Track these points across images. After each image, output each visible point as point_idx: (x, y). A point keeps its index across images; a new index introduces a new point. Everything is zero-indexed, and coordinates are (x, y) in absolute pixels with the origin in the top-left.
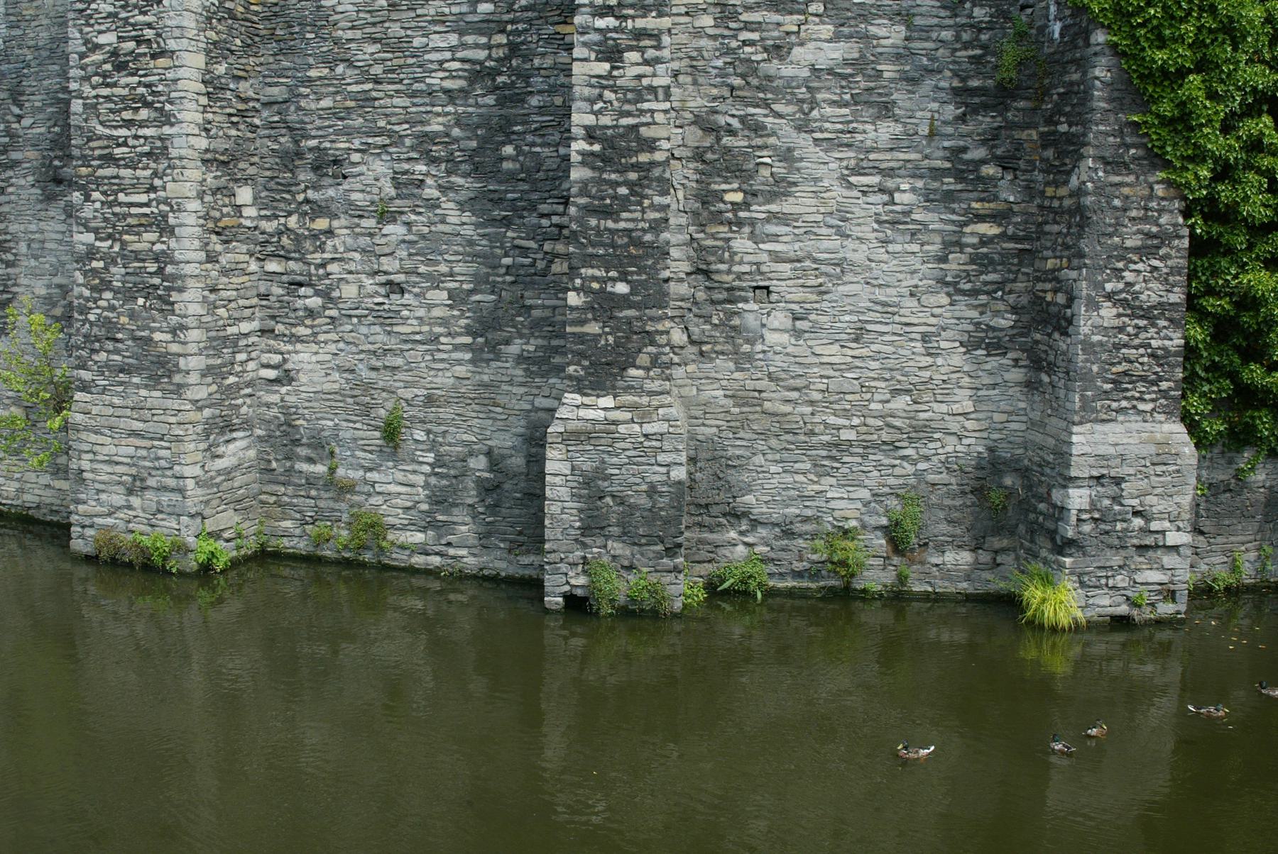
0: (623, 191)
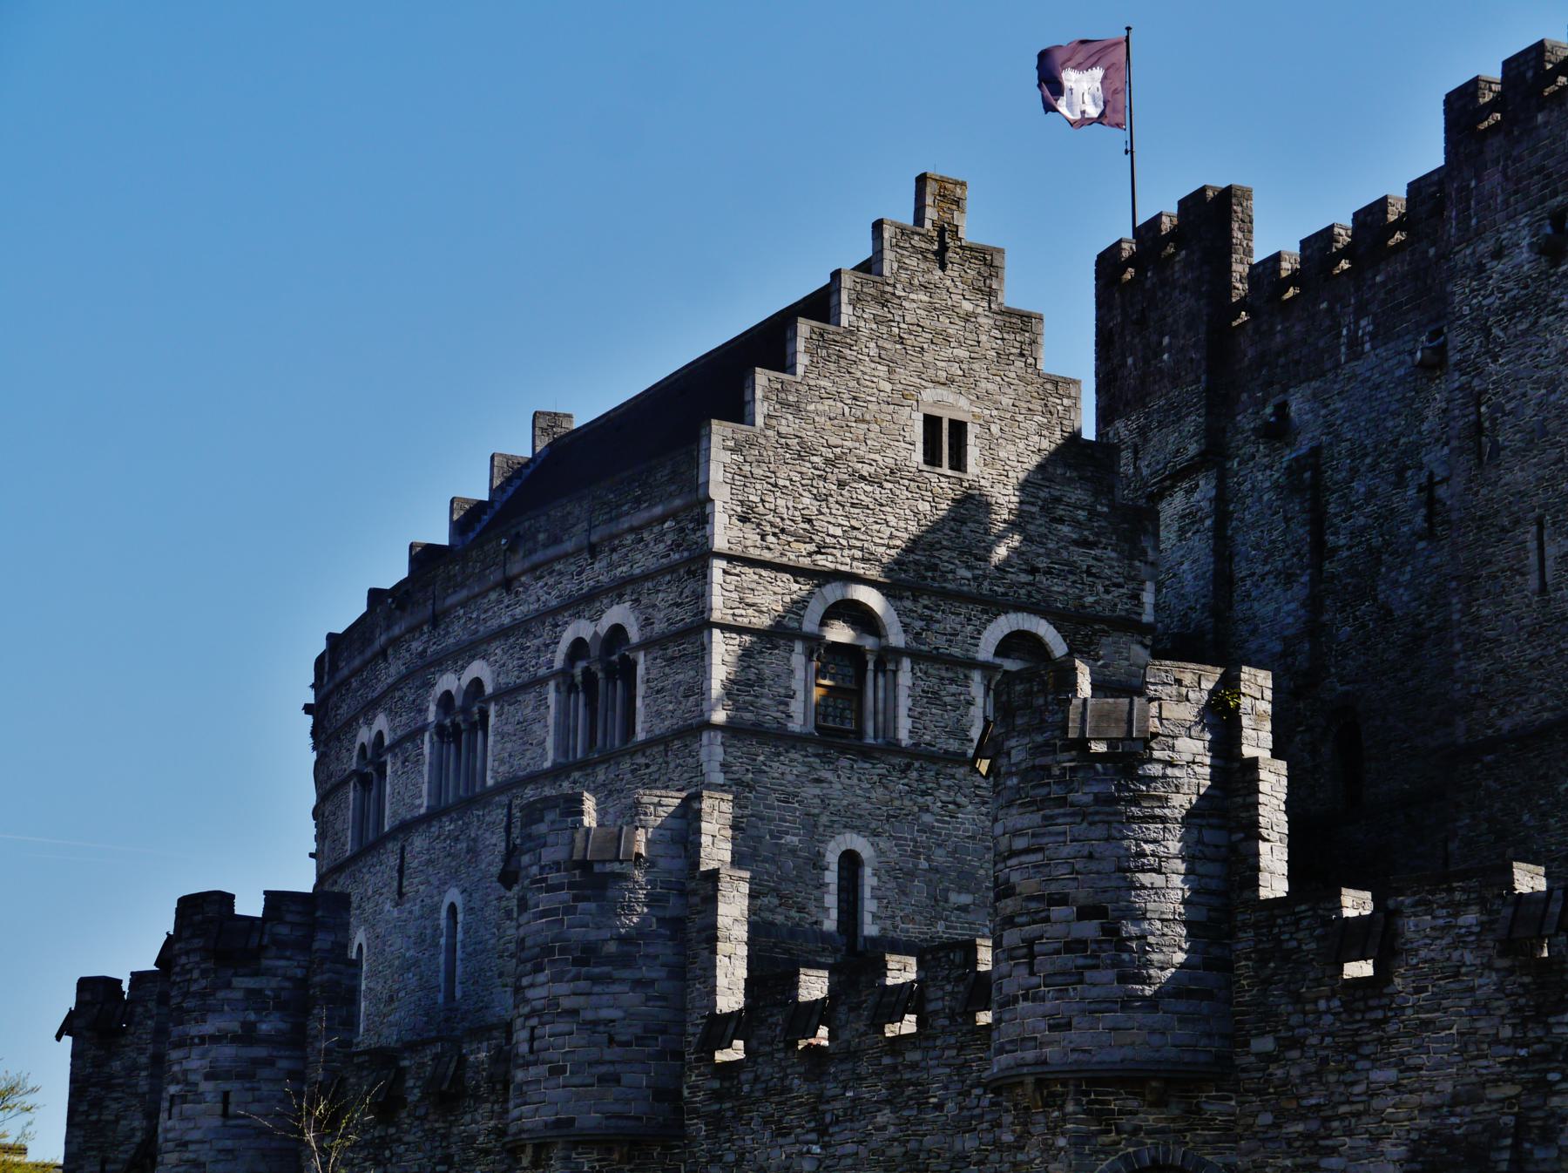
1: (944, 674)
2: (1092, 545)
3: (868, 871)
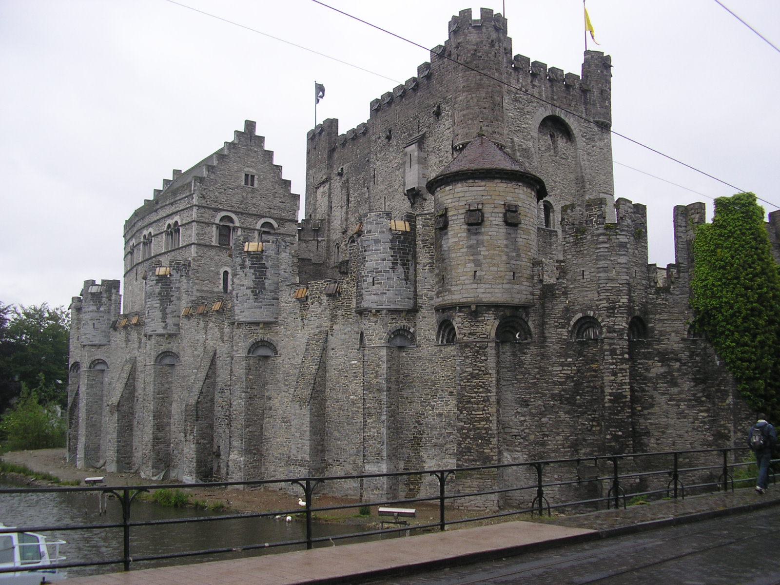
0: (619, 409)
2: (284, 203)
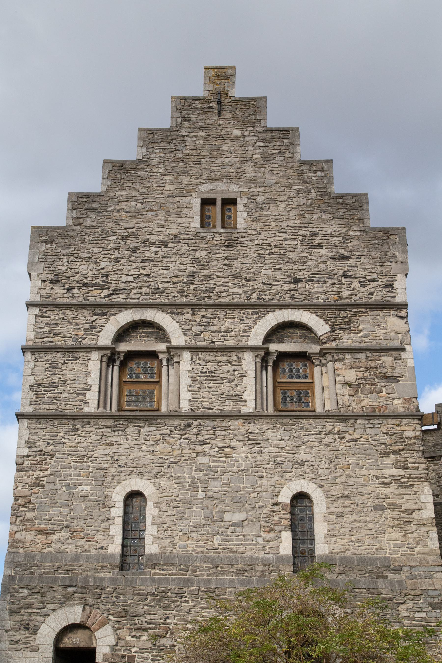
1: (219, 358)
3: (150, 504)
